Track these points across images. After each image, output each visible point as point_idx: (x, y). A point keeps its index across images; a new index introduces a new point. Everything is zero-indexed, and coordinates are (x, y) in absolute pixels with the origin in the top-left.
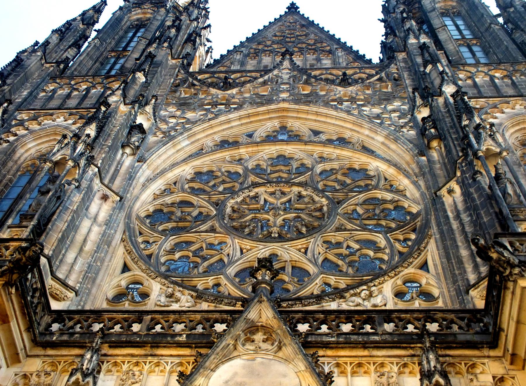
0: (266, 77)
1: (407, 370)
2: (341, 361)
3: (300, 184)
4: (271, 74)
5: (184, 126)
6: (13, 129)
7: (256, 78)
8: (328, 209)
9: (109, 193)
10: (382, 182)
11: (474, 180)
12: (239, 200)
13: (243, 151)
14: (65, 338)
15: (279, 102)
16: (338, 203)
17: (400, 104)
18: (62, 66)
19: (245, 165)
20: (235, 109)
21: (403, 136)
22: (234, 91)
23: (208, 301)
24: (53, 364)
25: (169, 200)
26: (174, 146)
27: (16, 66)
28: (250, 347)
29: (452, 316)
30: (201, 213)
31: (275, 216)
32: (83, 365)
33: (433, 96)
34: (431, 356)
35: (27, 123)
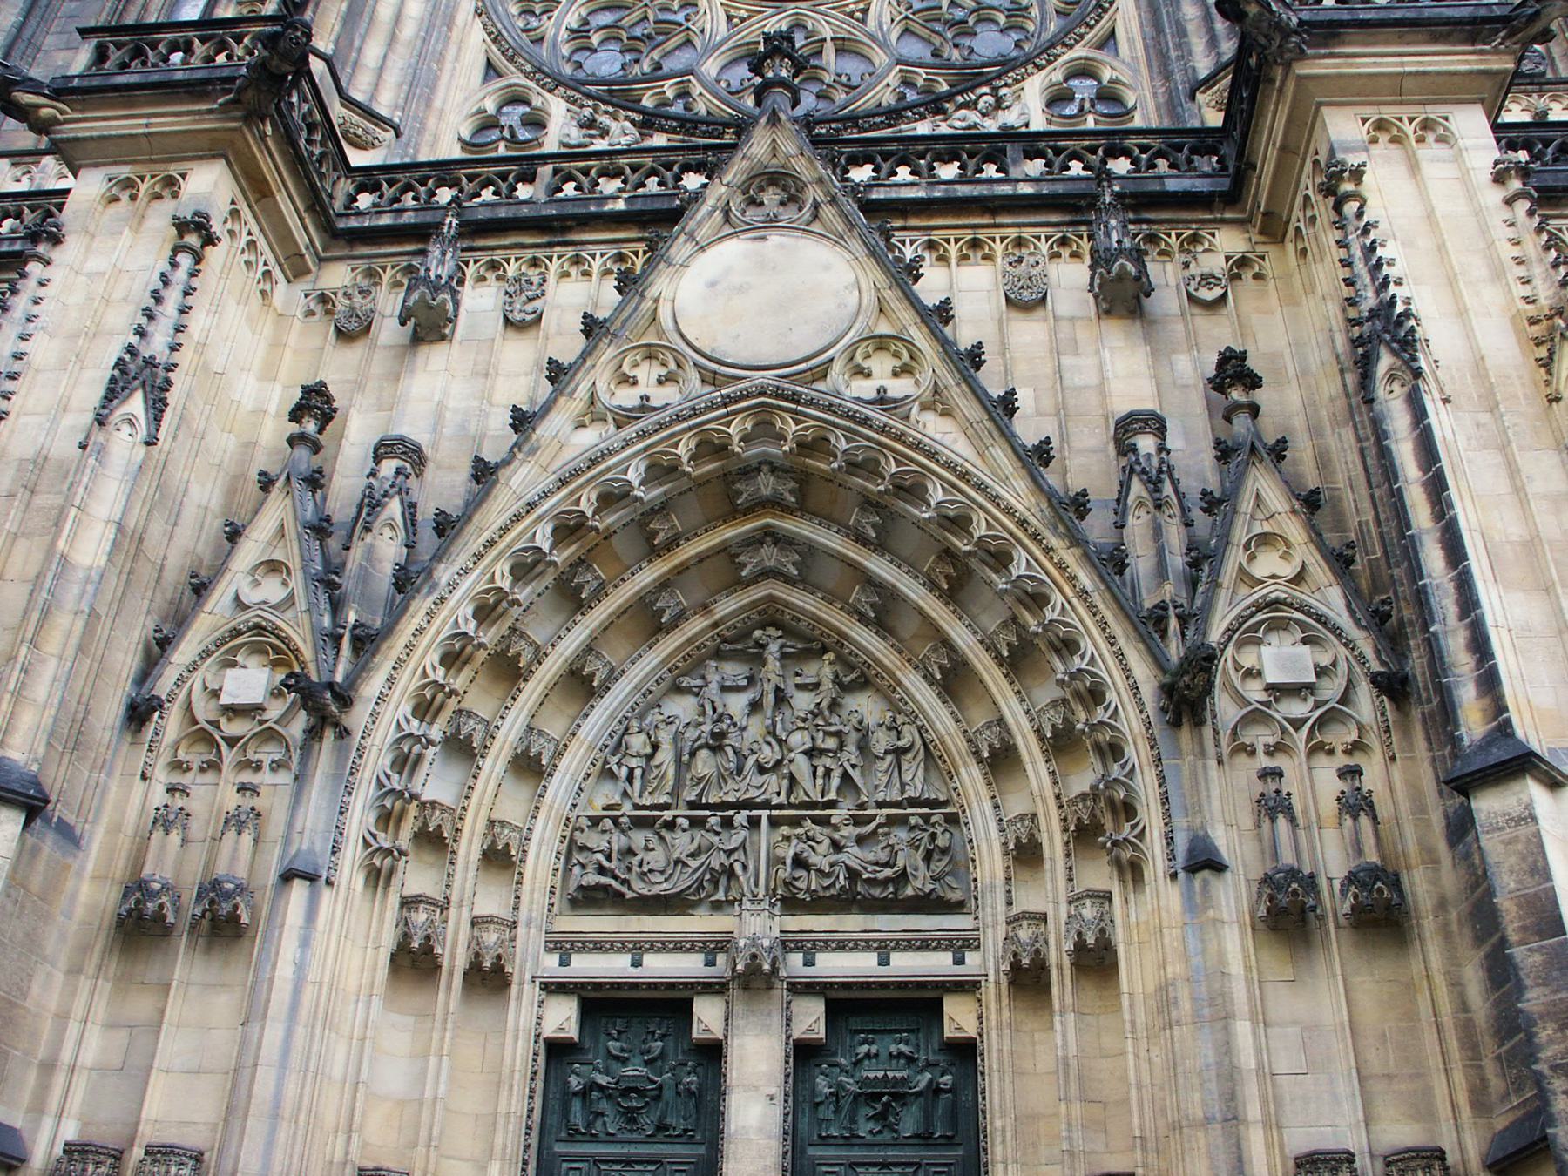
1: (1065, 252)
2: (936, 236)
14: (386, 220)
23: (666, 132)
24: (371, 273)
29: (1157, 144)
32: (428, 270)
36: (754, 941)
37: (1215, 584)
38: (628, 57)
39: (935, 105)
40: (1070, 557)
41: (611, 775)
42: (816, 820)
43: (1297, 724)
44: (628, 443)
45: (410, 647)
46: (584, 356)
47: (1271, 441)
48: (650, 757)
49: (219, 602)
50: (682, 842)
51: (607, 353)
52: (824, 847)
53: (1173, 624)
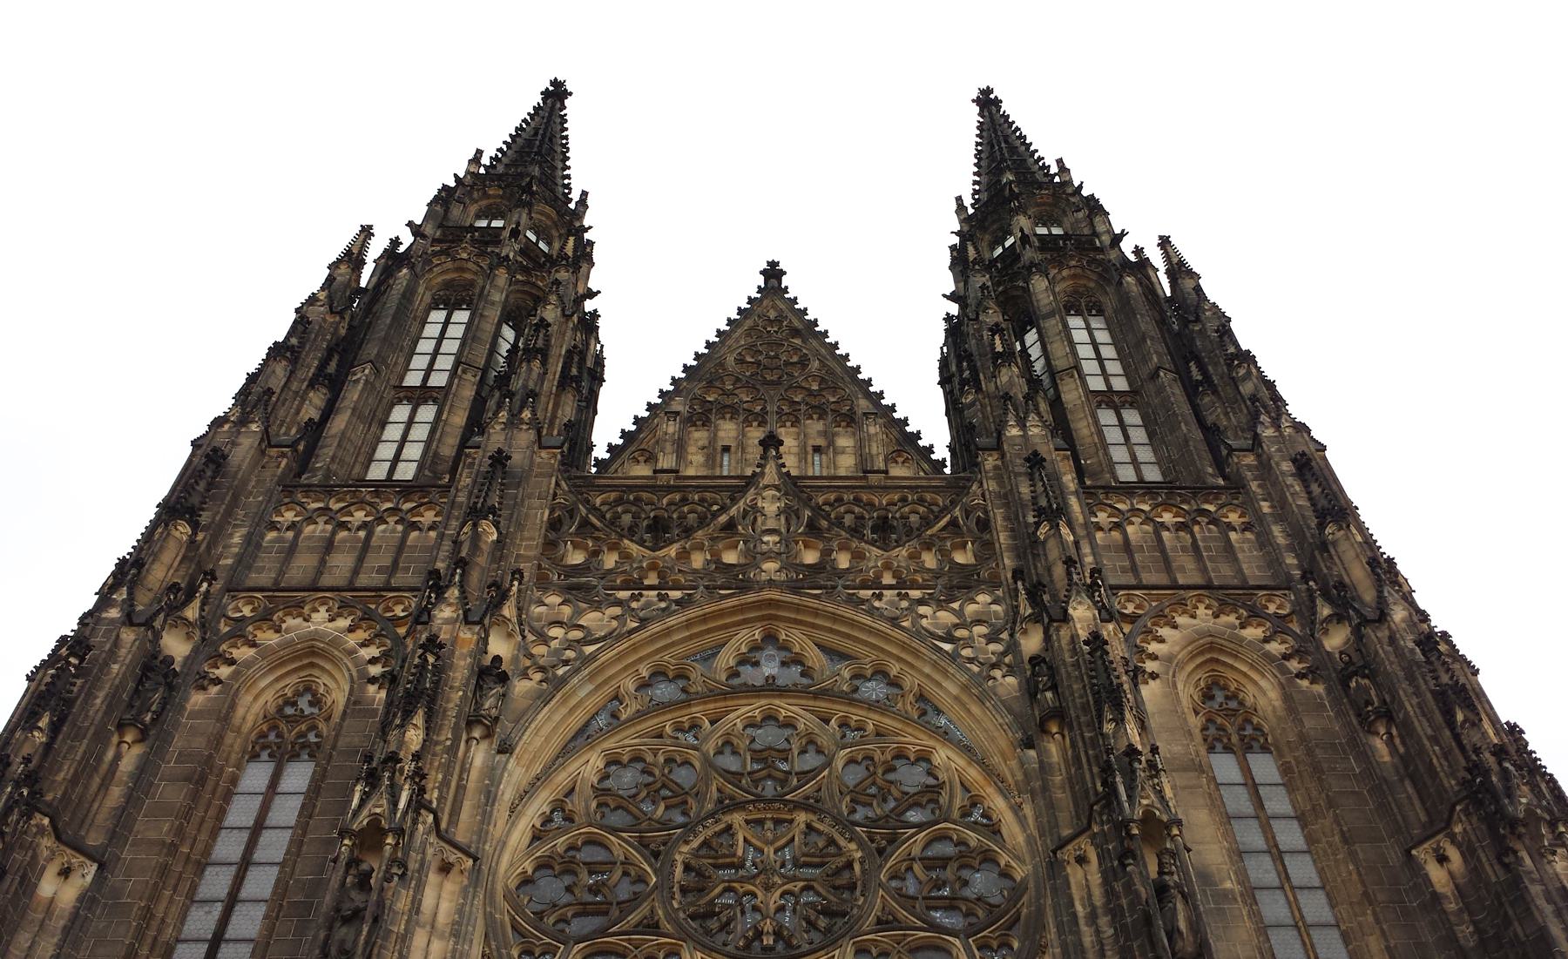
0: (733, 511)
5: (582, 652)
7: (715, 515)
8: (863, 871)
10: (958, 803)
12: (695, 844)
15: (761, 589)
16: (881, 852)
17: (988, 599)
18: (301, 448)
19: (704, 748)
20: (678, 602)
21: (993, 688)
22: (673, 551)
25: (561, 842)
26: (565, 700)
30: (626, 874)
31: (768, 888)
33: (1052, 620)
35: (250, 628)
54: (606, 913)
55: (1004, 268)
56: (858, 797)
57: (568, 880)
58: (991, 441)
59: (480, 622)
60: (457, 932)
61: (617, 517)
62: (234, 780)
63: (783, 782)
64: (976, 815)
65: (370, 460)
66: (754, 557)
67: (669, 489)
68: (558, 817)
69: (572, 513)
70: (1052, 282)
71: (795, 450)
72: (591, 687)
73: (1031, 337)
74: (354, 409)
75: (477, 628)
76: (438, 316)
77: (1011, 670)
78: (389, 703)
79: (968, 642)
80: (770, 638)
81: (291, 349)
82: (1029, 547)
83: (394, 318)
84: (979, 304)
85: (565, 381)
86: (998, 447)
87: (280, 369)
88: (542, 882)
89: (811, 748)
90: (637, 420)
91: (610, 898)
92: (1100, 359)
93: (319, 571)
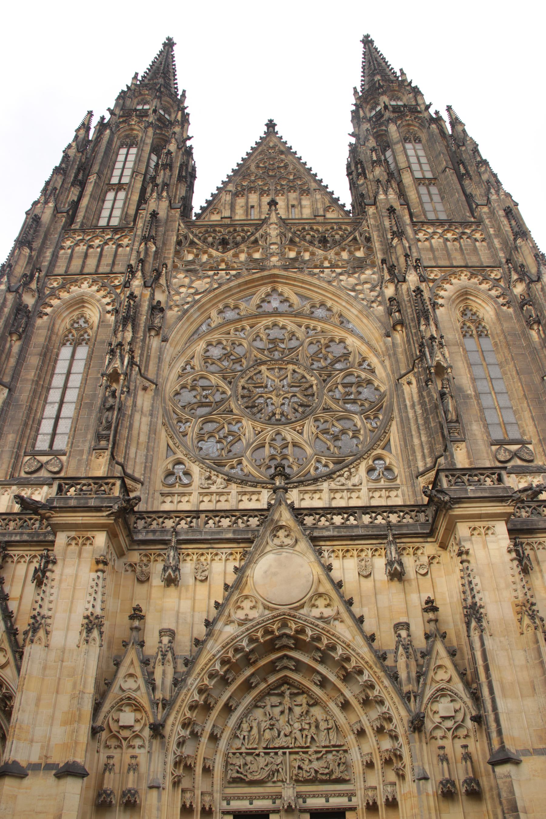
0: (257, 235)
1: (377, 553)
2: (335, 548)
3: (294, 363)
4: (261, 232)
6: (47, 300)
7: (249, 237)
8: (317, 389)
9: (147, 384)
11: (427, 385)
12: (247, 378)
13: (244, 323)
18: (70, 213)
20: (234, 276)
22: (231, 252)
24: (146, 555)
27: (37, 226)
28: (277, 541)
29: (407, 510)
33: (399, 282)
34: (393, 548)
36: (290, 797)
37: (425, 684)
38: (219, 446)
39: (329, 476)
40: (381, 674)
41: (238, 737)
42: (304, 753)
43: (449, 729)
44: (243, 633)
45: (180, 706)
46: (227, 599)
47: (441, 633)
48: (250, 731)
49: (115, 689)
50: (262, 761)
51: (235, 598)
52: (307, 762)
53: (412, 699)
54: (211, 406)
55: (377, 121)
56: (314, 357)
57: (194, 393)
58: (372, 201)
59: (151, 286)
60: (151, 415)
61: (206, 238)
62: (58, 355)
63: (283, 353)
64: (365, 365)
65: (99, 217)
66: (267, 256)
67: (228, 226)
68: (188, 367)
69: (186, 237)
70: (398, 127)
71: (283, 207)
72: (199, 313)
73: (388, 153)
74: (91, 195)
75: (149, 289)
76: (123, 151)
77: (380, 303)
78: (116, 322)
79: (361, 291)
80: (274, 290)
81: (63, 169)
82: (388, 248)
83: (105, 153)
84: (365, 138)
85: (180, 178)
86: (375, 204)
87: (59, 179)
88: (183, 394)
89: (294, 338)
90: (212, 195)
91: (212, 400)
92: (420, 163)
93: (83, 267)
